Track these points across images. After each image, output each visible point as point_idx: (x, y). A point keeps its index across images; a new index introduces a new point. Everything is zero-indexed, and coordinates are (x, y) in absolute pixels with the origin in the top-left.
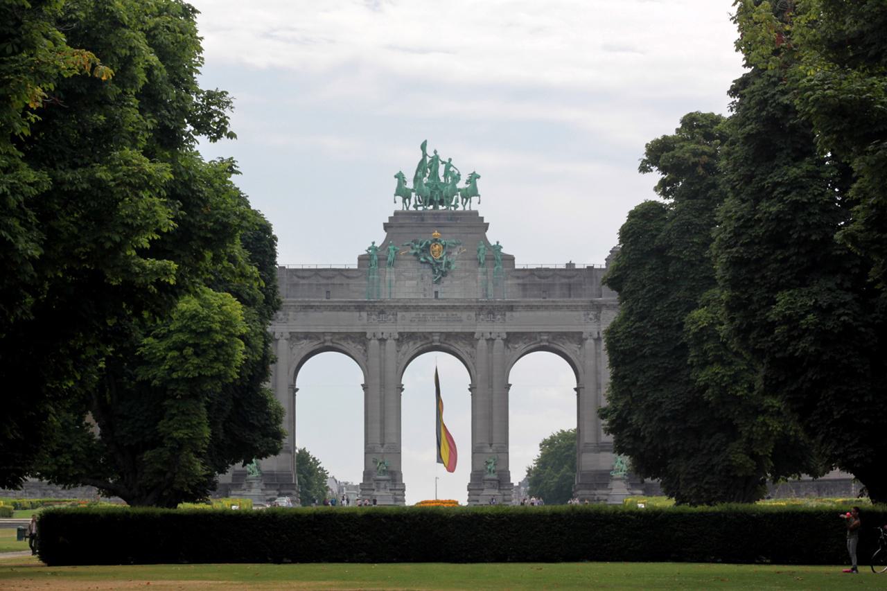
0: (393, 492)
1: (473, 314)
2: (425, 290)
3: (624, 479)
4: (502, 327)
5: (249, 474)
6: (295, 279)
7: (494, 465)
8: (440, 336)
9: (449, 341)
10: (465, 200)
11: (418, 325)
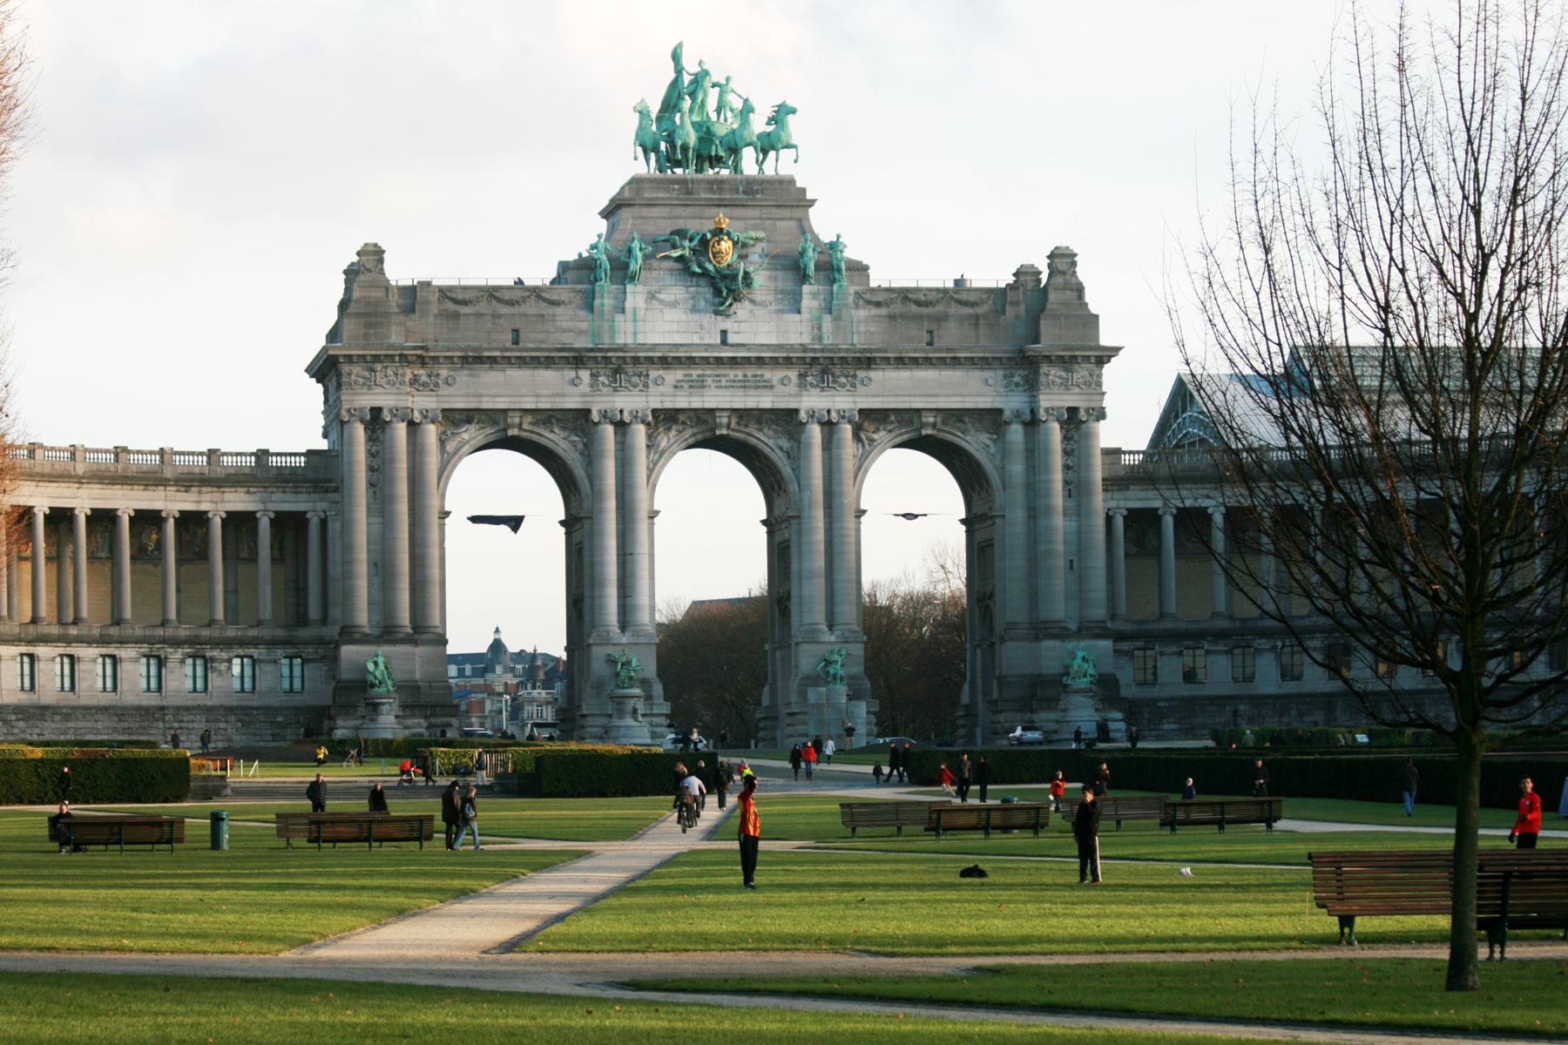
0: (648, 719)
1: (793, 374)
2: (701, 327)
3: (1091, 691)
4: (848, 399)
5: (373, 685)
6: (451, 306)
7: (842, 665)
8: (729, 417)
9: (746, 426)
10: (761, 156)
11: (690, 395)
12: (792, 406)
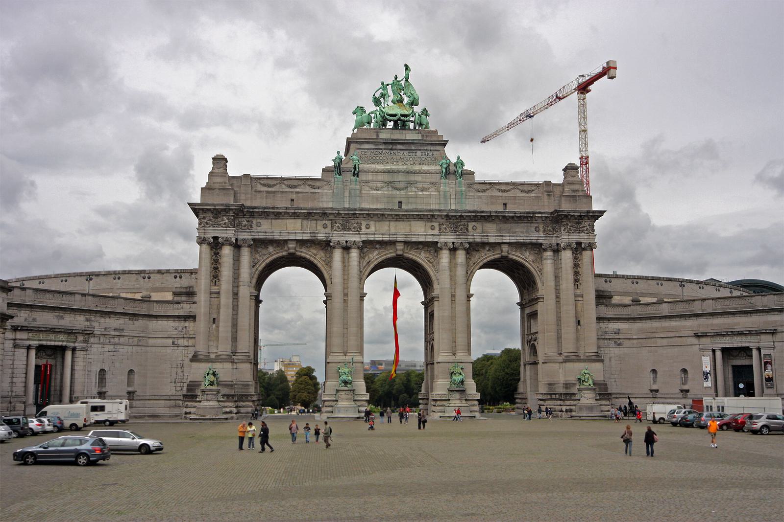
1: (436, 224)
12: (435, 240)
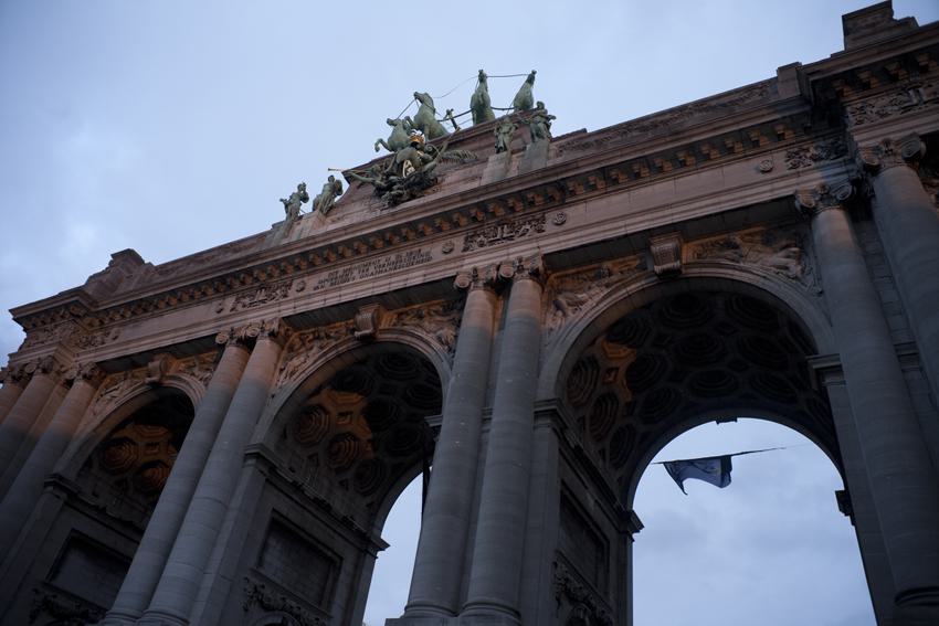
1: (459, 242)
4: (529, 246)
9: (404, 325)
